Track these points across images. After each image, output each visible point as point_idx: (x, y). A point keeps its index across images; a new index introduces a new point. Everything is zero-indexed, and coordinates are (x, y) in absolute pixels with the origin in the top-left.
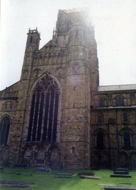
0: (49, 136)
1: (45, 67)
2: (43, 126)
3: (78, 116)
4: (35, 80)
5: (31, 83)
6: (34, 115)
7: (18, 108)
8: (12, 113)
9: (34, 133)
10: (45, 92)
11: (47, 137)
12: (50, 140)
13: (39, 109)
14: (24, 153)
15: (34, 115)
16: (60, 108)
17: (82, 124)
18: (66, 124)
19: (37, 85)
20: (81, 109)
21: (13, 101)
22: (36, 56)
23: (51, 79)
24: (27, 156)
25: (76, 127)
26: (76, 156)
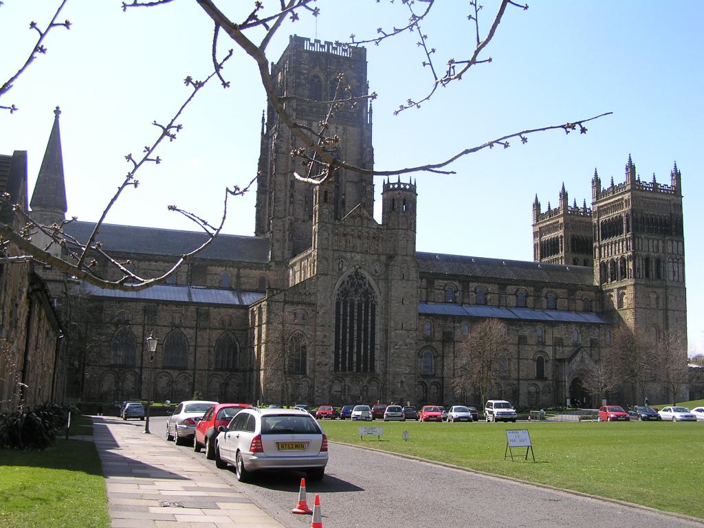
0: (365, 365)
1: (353, 254)
2: (355, 350)
3: (408, 341)
4: (339, 277)
5: (334, 282)
6: (341, 333)
7: (319, 321)
8: (308, 329)
9: (344, 361)
10: (356, 299)
11: (362, 366)
12: (367, 371)
13: (348, 325)
14: (331, 388)
15: (341, 333)
16: (378, 327)
17: (412, 352)
18: (392, 351)
19: (341, 285)
20: (411, 332)
21: (307, 308)
22: (337, 231)
23: (363, 278)
24: (336, 391)
25: (405, 355)
26: (405, 391)
